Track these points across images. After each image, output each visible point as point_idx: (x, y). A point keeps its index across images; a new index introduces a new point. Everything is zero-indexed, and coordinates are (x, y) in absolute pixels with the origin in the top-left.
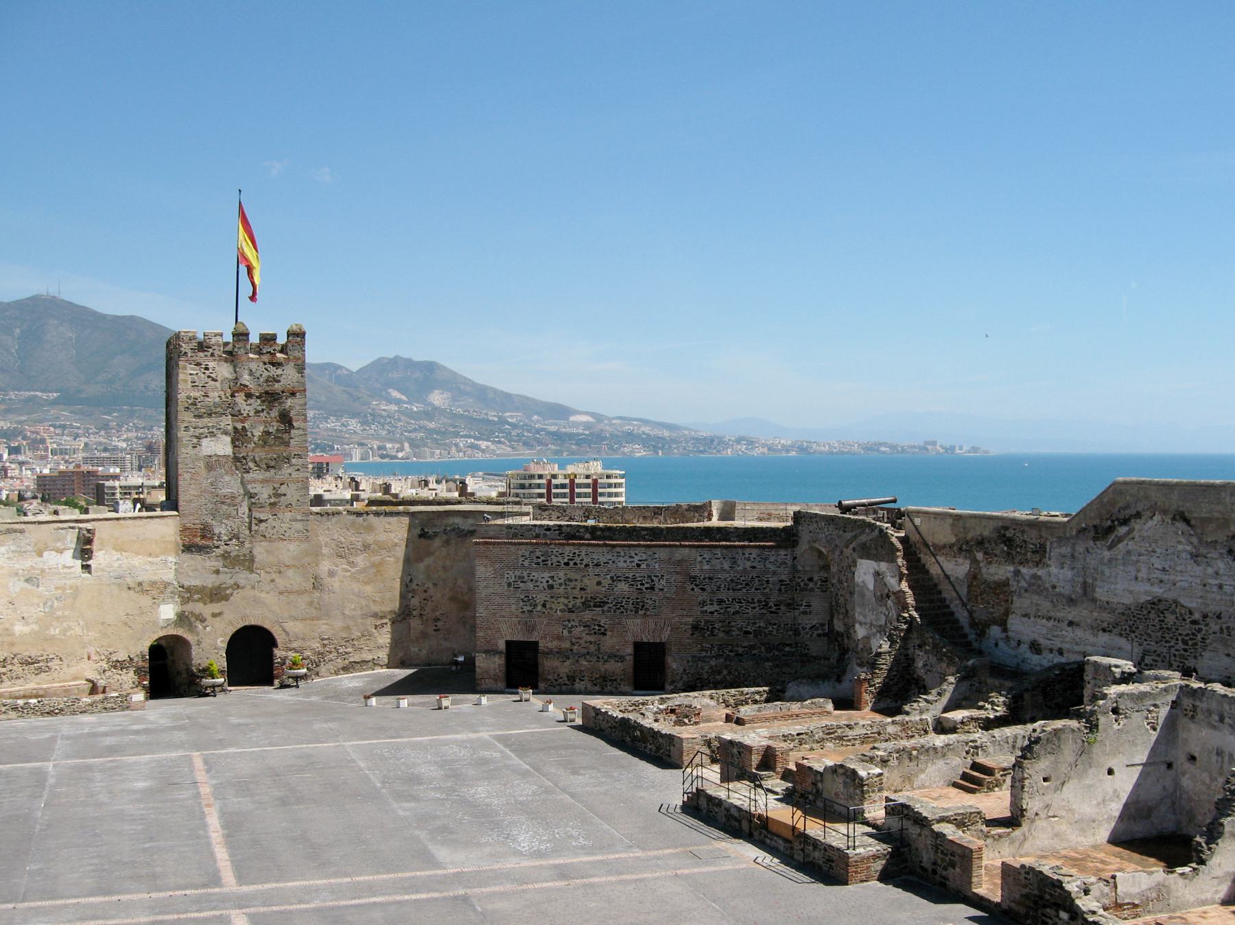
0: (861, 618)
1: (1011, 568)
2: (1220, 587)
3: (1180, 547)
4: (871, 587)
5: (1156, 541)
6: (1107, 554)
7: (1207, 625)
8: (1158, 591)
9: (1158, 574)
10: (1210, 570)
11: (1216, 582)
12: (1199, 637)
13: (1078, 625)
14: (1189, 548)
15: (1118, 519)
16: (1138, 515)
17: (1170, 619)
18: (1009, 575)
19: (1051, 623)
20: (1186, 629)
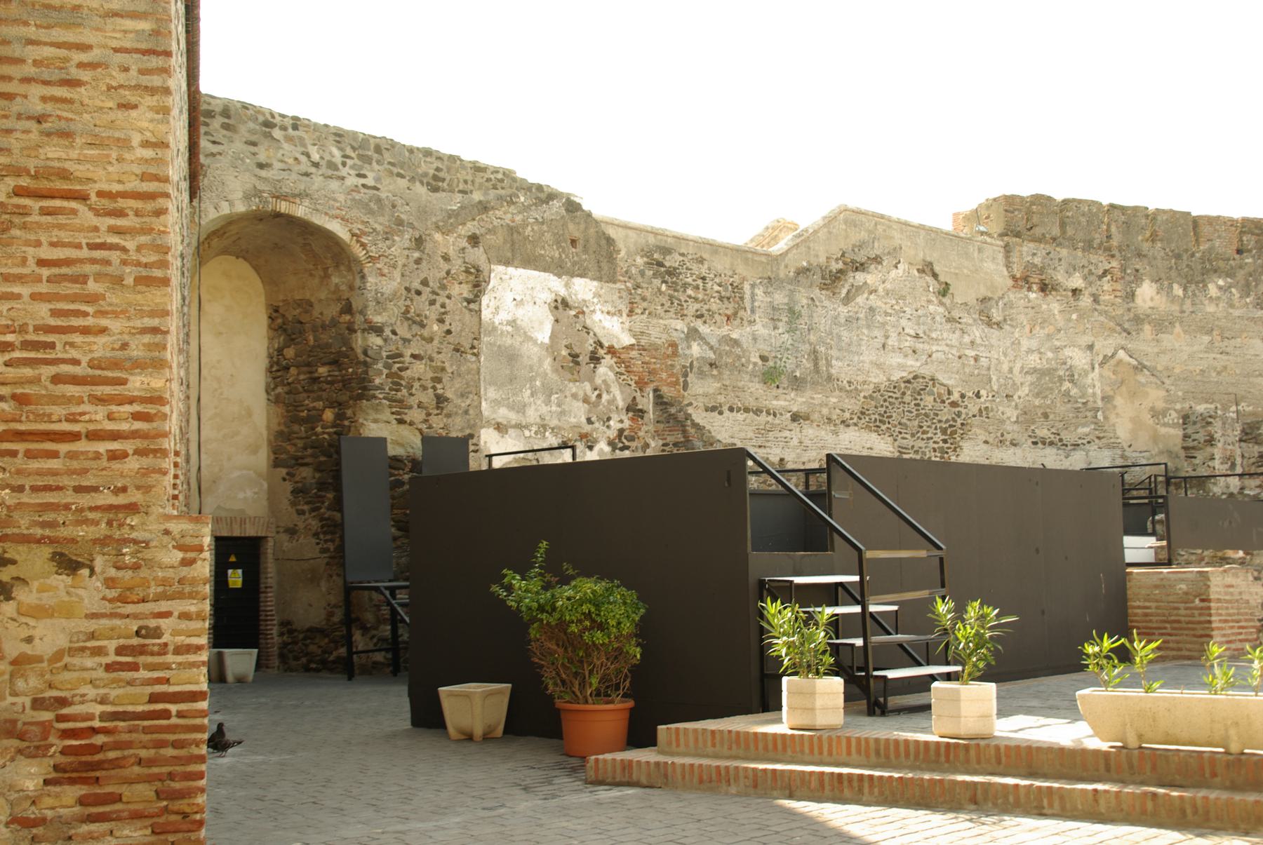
0: (503, 414)
1: (680, 325)
2: (976, 359)
3: (931, 308)
4: (544, 336)
5: (903, 298)
6: (843, 310)
7: (966, 407)
8: (913, 364)
9: (909, 342)
10: (967, 339)
11: (973, 353)
12: (959, 421)
13: (807, 418)
14: (941, 310)
15: (853, 261)
16: (877, 260)
17: (928, 401)
18: (676, 336)
19: (763, 418)
20: (946, 414)
